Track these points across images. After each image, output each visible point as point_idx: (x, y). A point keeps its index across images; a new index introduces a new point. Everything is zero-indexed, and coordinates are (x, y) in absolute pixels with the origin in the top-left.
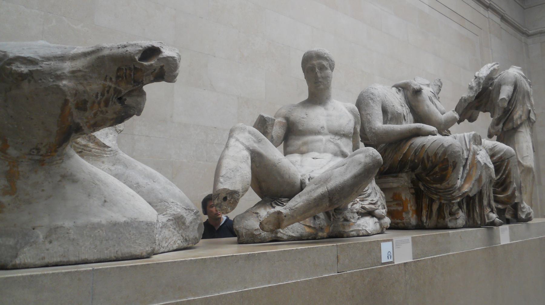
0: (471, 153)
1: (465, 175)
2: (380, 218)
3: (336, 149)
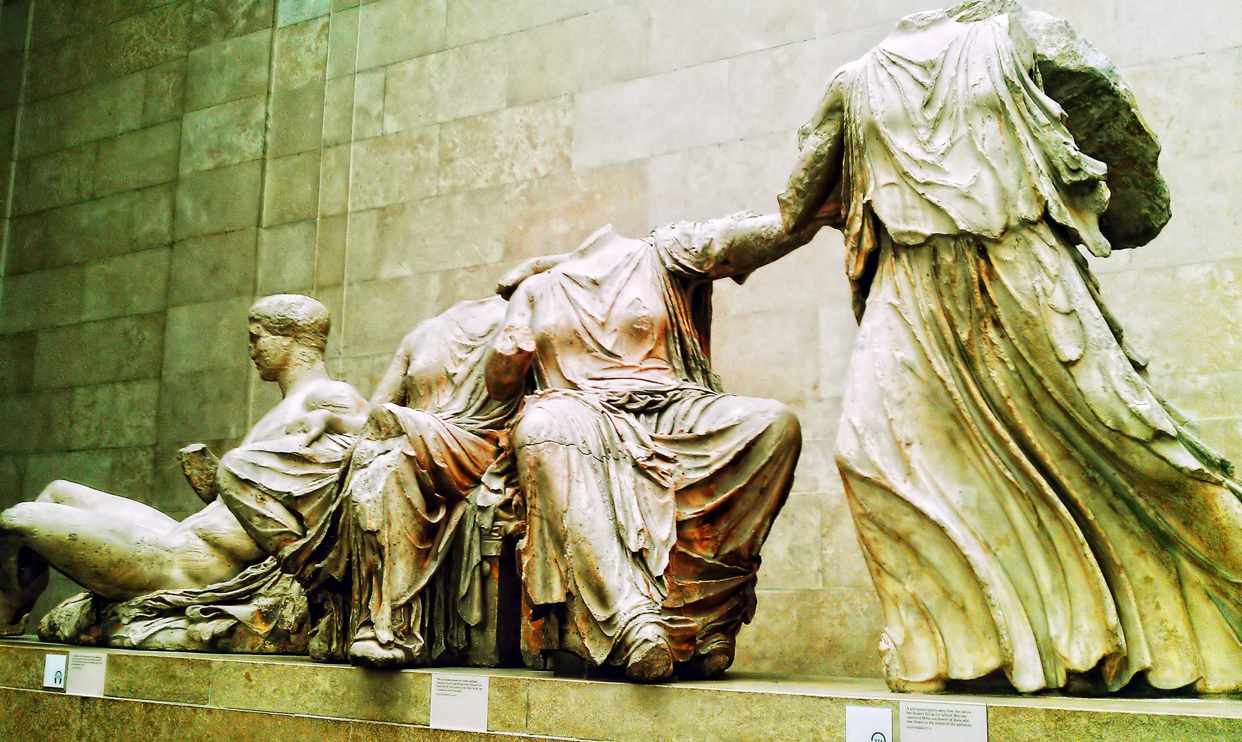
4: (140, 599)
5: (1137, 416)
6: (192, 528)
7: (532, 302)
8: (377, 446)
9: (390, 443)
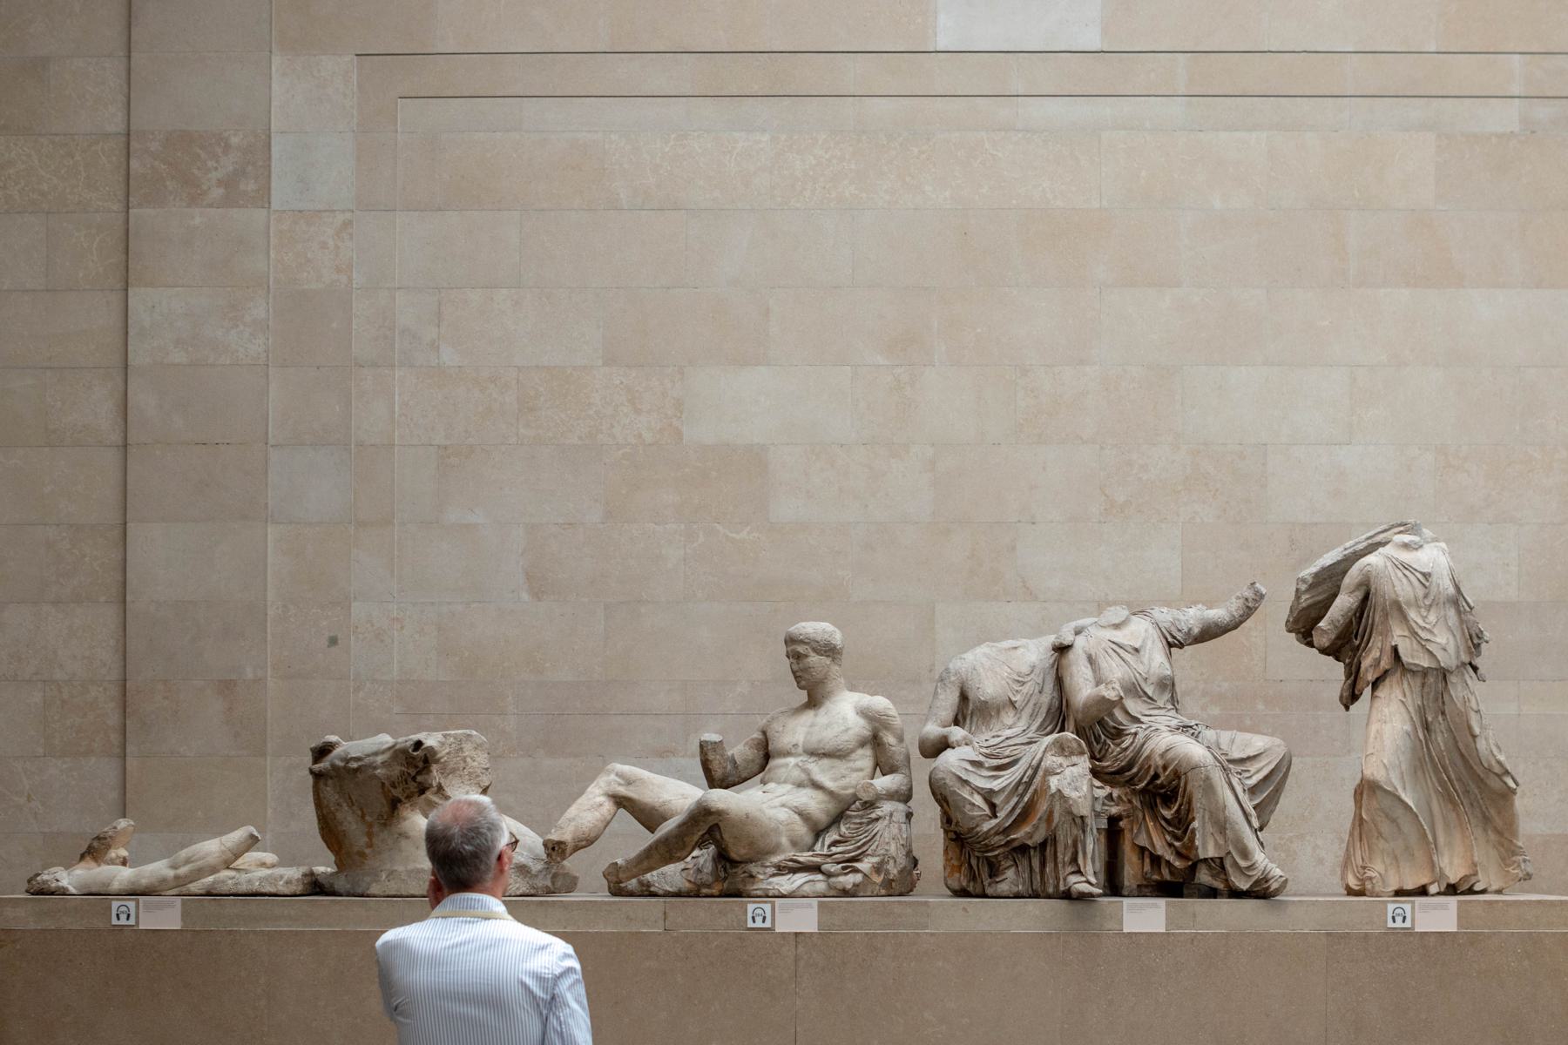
0: (1040, 773)
1: (1018, 811)
2: (829, 875)
3: (803, 776)
4: (776, 859)
5: (1499, 762)
6: (783, 806)
7: (1091, 660)
8: (1060, 760)
9: (1075, 759)
